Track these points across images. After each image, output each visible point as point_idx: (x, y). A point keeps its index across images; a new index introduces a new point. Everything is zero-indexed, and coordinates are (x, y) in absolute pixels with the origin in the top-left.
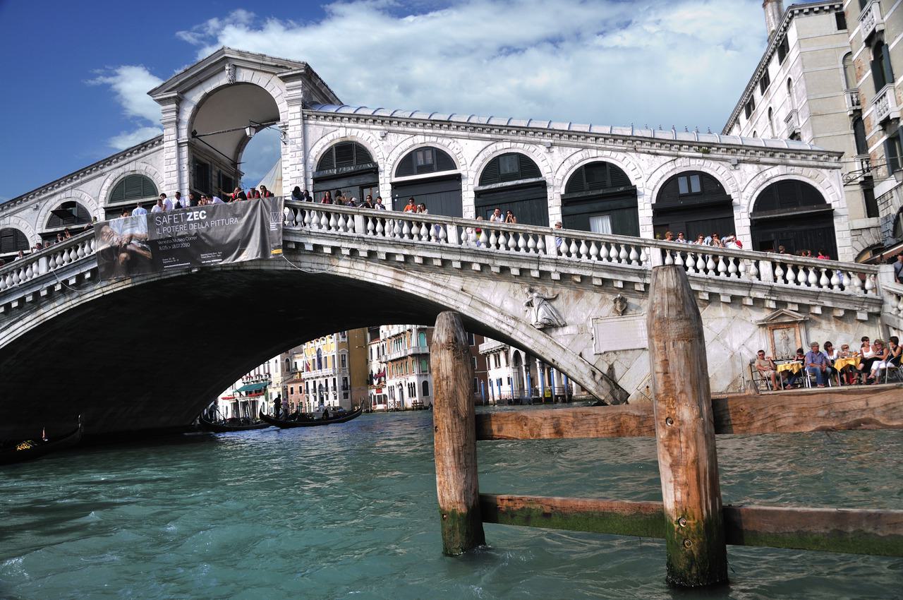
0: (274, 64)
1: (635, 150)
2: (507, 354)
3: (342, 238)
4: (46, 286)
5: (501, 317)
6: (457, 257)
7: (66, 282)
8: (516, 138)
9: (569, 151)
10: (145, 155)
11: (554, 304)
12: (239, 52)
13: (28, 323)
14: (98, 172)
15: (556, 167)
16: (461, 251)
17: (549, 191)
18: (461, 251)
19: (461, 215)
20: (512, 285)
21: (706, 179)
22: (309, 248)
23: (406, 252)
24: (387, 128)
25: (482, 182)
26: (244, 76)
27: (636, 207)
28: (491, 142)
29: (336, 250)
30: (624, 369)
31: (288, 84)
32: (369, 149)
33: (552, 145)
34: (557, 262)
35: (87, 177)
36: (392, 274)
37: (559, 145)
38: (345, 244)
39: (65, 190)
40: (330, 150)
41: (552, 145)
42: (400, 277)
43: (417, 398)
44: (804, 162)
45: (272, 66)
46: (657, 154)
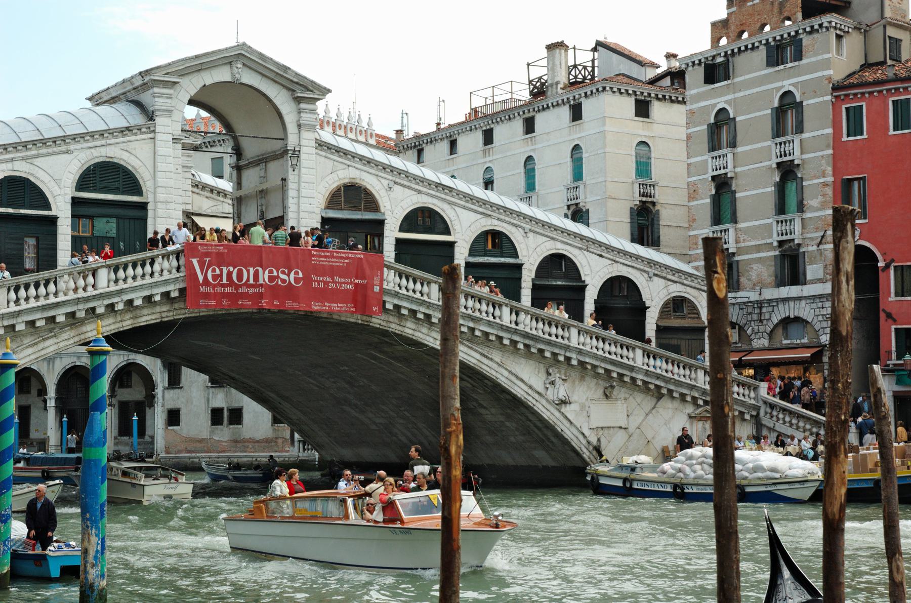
0: (295, 80)
5: (530, 391)
6: (509, 336)
8: (502, 217)
10: (127, 142)
12: (262, 56)
14: (64, 148)
15: (531, 252)
16: (516, 332)
17: (525, 273)
19: (518, 300)
22: (389, 306)
23: (471, 325)
24: (394, 179)
26: (249, 78)
27: (582, 300)
29: (413, 312)
31: (302, 106)
33: (530, 230)
37: (535, 232)
38: (423, 309)
39: (12, 160)
40: (338, 189)
41: (530, 230)
44: (693, 284)
45: (292, 81)
46: (601, 256)
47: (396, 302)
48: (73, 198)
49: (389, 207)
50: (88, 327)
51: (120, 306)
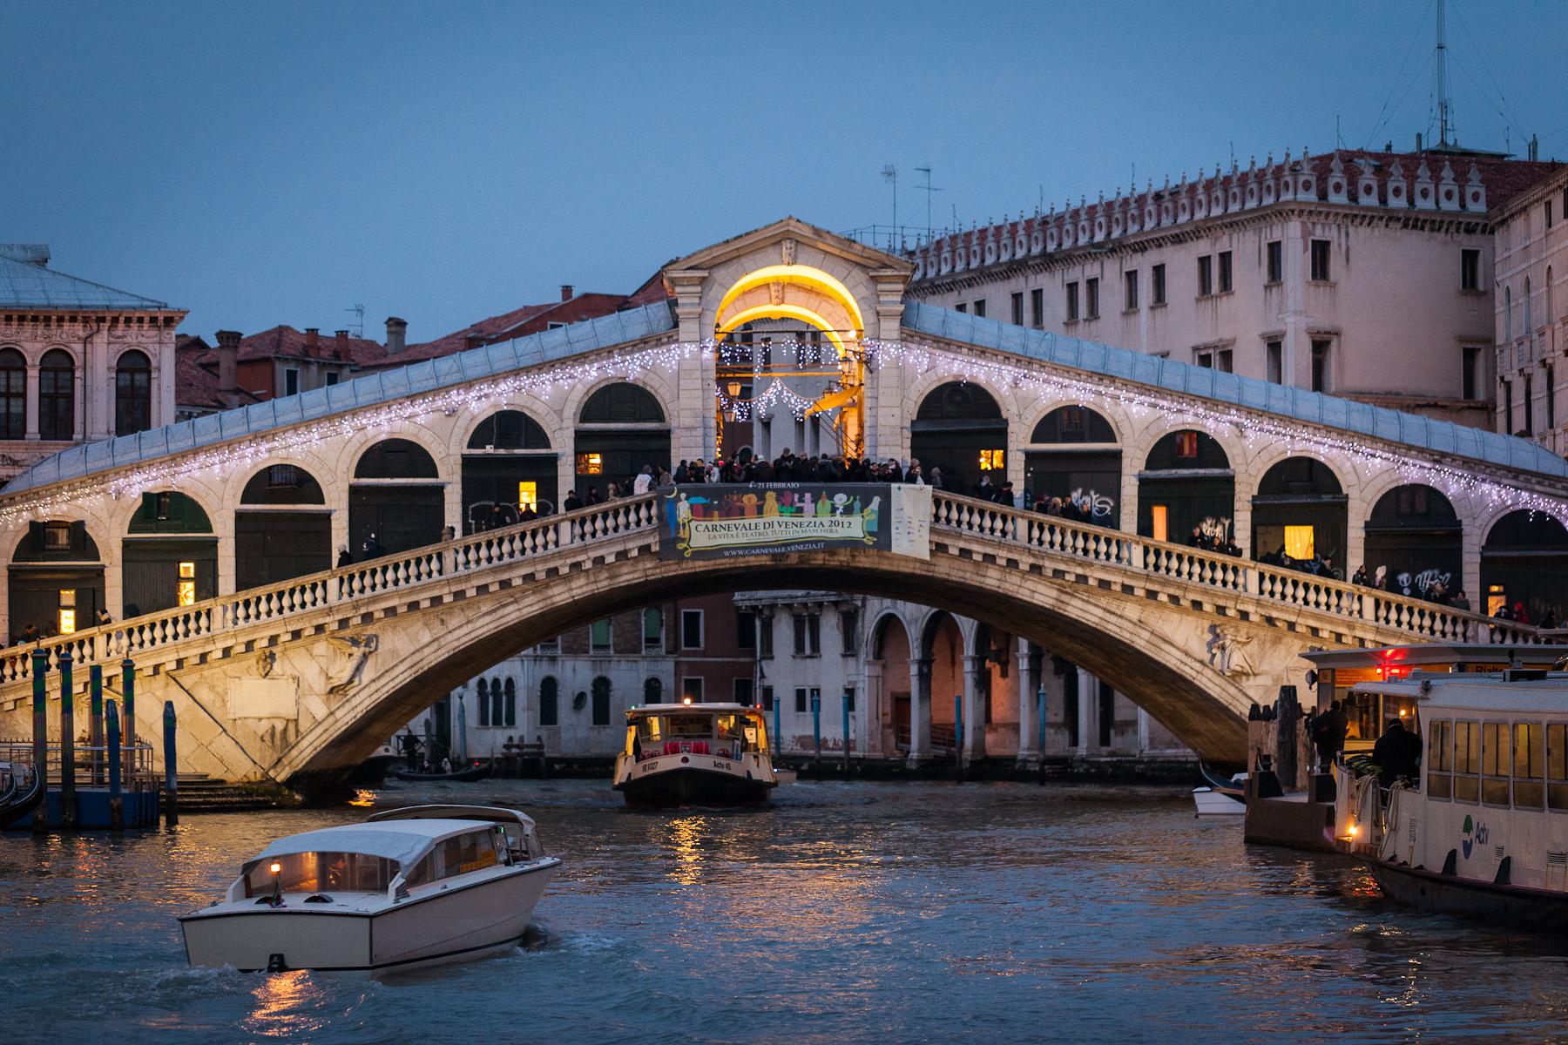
2: (849, 622)
3: (1000, 545)
4: (569, 561)
5: (1185, 659)
6: (1142, 584)
11: (1248, 647)
13: (529, 607)
17: (1237, 488)
18: (1148, 578)
21: (1433, 496)
22: (954, 551)
23: (1080, 571)
25: (1151, 463)
31: (880, 287)
34: (1258, 603)
36: (1054, 593)
42: (1065, 598)
43: (525, 726)
47: (962, 544)
48: (576, 432)
49: (1014, 409)
50: (556, 590)
51: (588, 565)
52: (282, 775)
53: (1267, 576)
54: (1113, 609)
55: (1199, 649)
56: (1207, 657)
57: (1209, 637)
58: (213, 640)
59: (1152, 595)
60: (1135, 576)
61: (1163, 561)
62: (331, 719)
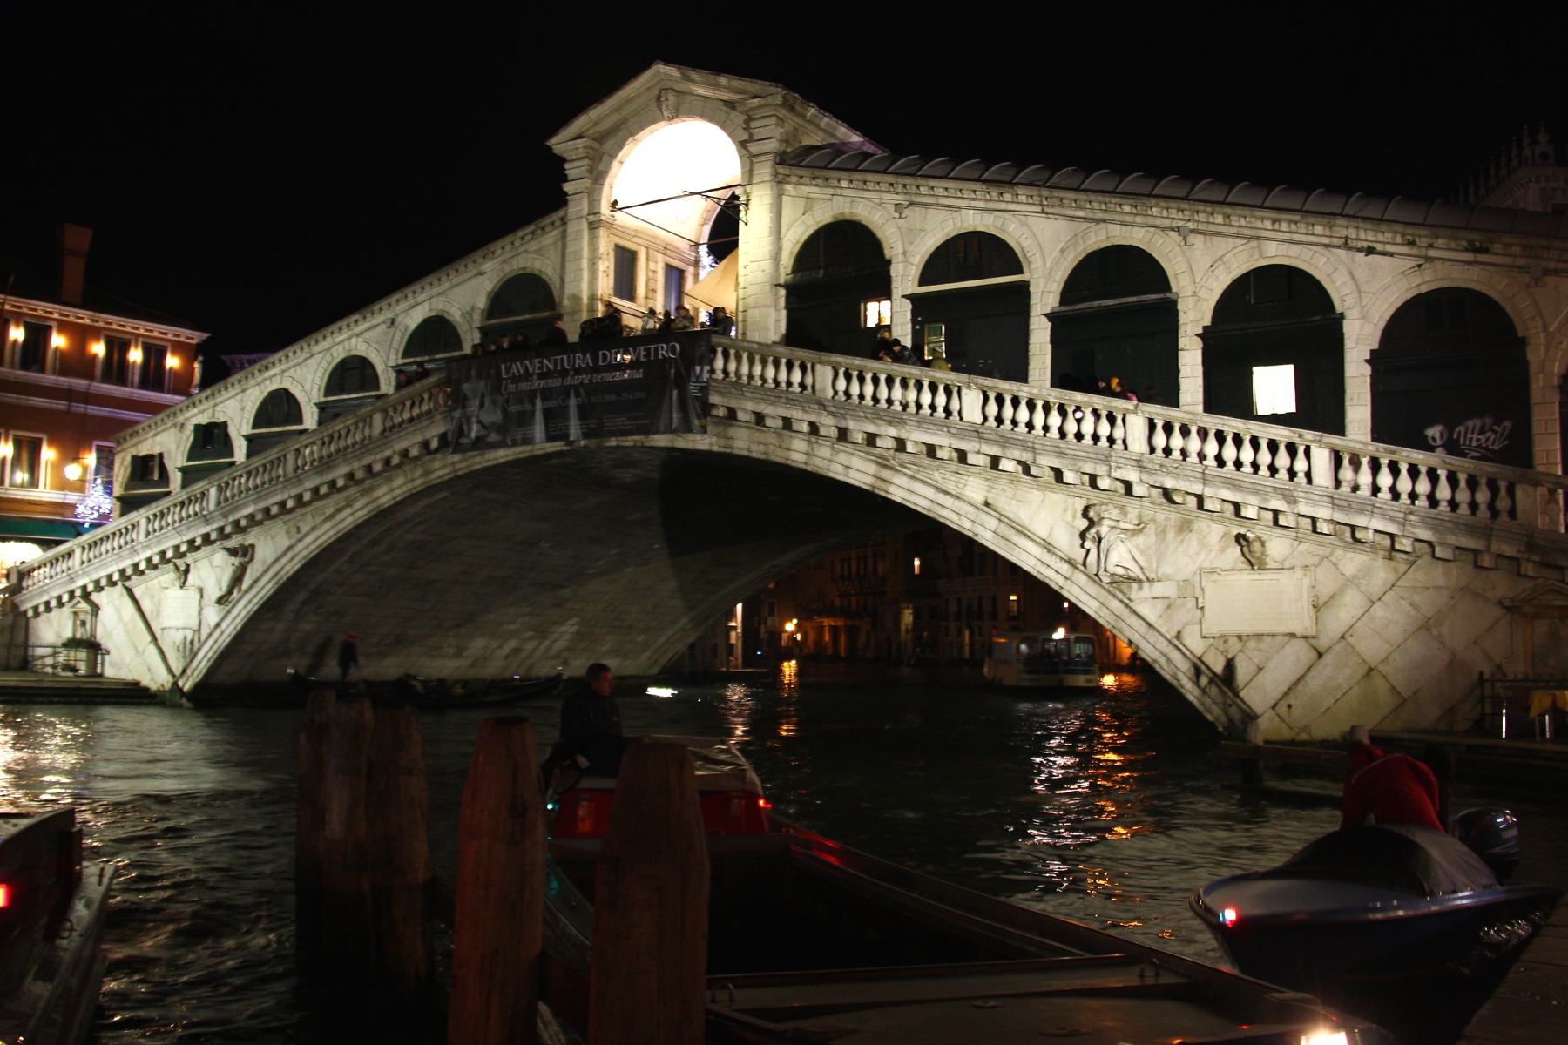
1: (1346, 246)
5: (1047, 557)
7: (405, 454)
8: (1128, 219)
9: (1222, 245)
20: (1070, 500)
28: (1086, 225)
30: (1252, 668)
32: (879, 234)
34: (1139, 464)
35: (461, 278)
36: (872, 468)
37: (1204, 233)
38: (795, 414)
42: (886, 474)
50: (380, 491)
52: (187, 685)
53: (1160, 424)
54: (950, 486)
55: (1067, 541)
56: (1079, 555)
57: (1084, 524)
58: (135, 552)
59: (995, 462)
60: (961, 434)
61: (1008, 411)
62: (218, 631)
